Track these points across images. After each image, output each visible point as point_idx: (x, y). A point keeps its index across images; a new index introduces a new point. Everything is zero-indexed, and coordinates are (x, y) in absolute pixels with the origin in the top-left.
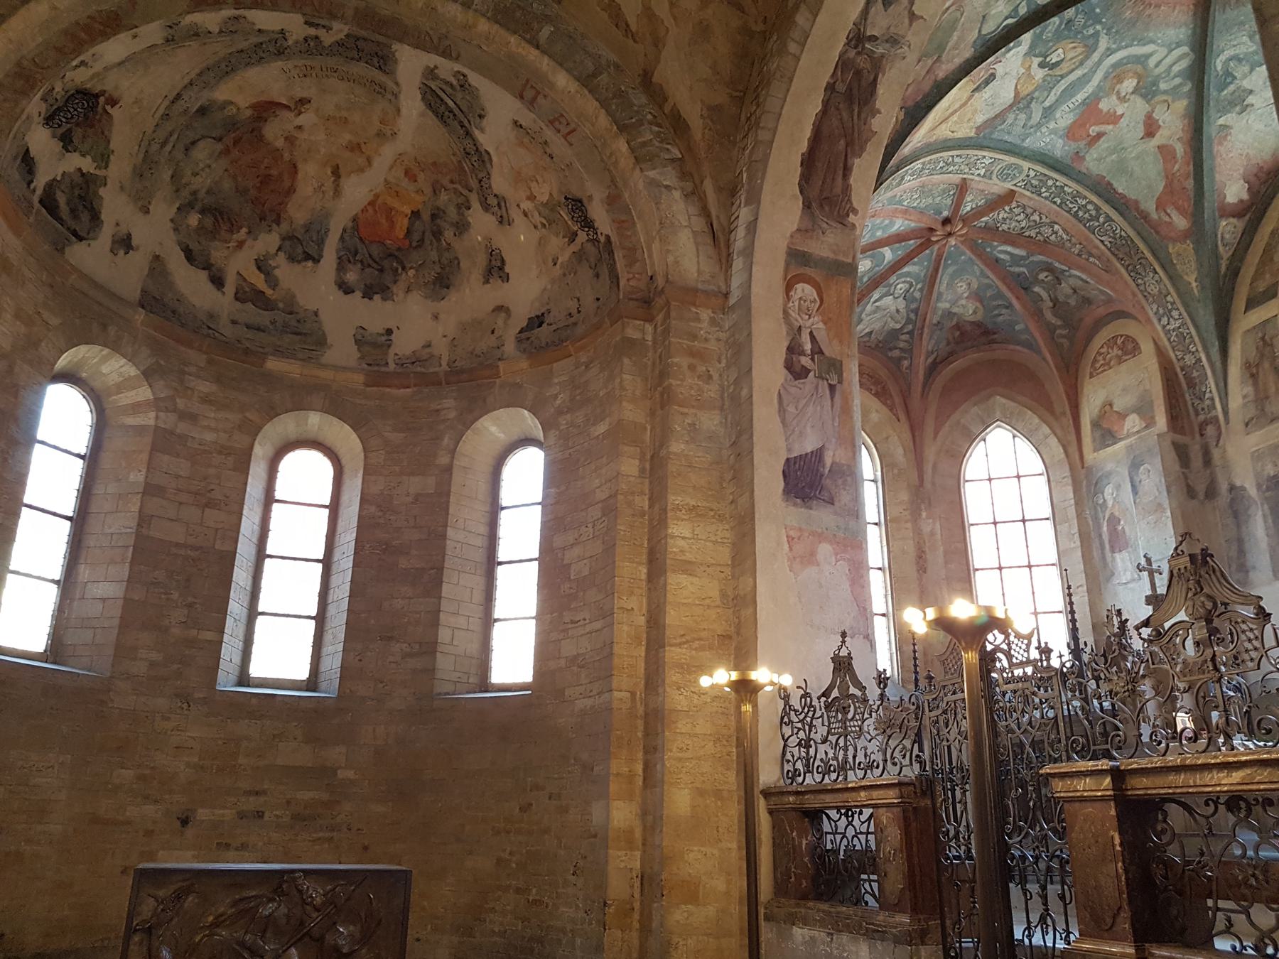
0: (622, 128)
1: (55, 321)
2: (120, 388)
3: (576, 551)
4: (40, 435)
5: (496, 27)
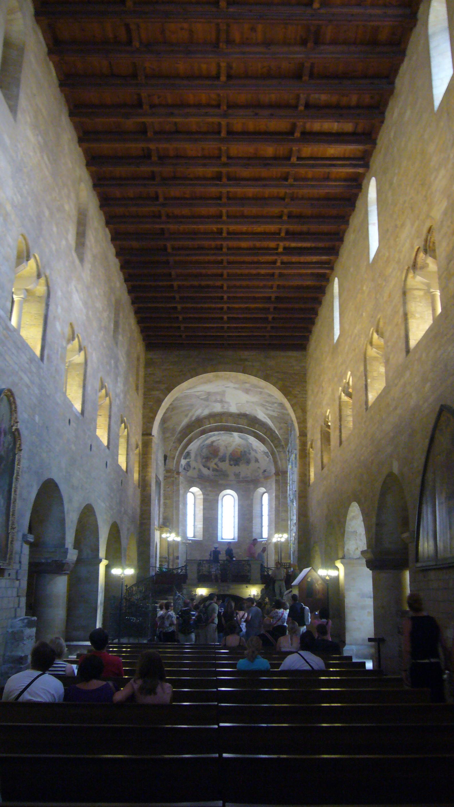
0: (272, 442)
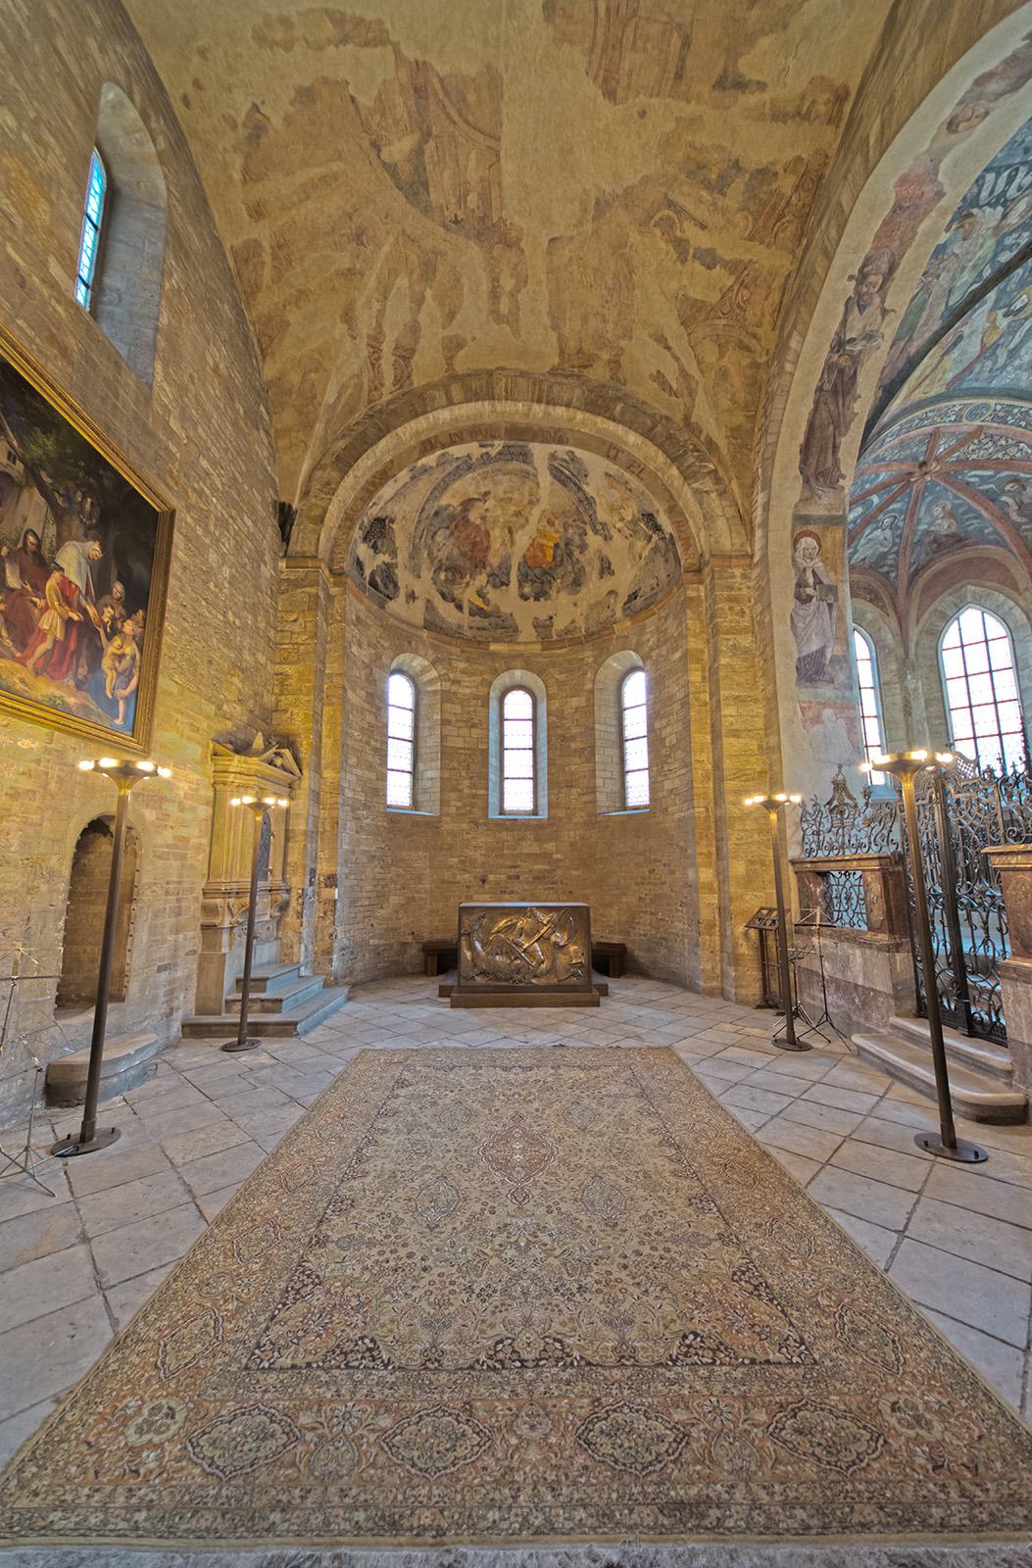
0: (674, 460)
1: (387, 644)
2: (424, 671)
3: (669, 730)
4: (391, 702)
5: (587, 415)
